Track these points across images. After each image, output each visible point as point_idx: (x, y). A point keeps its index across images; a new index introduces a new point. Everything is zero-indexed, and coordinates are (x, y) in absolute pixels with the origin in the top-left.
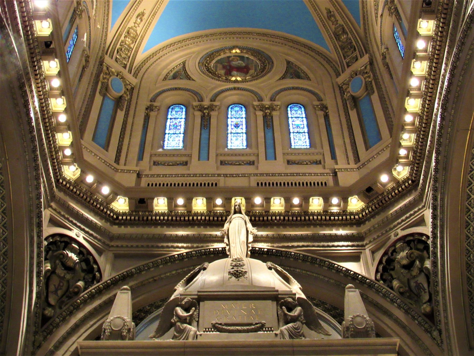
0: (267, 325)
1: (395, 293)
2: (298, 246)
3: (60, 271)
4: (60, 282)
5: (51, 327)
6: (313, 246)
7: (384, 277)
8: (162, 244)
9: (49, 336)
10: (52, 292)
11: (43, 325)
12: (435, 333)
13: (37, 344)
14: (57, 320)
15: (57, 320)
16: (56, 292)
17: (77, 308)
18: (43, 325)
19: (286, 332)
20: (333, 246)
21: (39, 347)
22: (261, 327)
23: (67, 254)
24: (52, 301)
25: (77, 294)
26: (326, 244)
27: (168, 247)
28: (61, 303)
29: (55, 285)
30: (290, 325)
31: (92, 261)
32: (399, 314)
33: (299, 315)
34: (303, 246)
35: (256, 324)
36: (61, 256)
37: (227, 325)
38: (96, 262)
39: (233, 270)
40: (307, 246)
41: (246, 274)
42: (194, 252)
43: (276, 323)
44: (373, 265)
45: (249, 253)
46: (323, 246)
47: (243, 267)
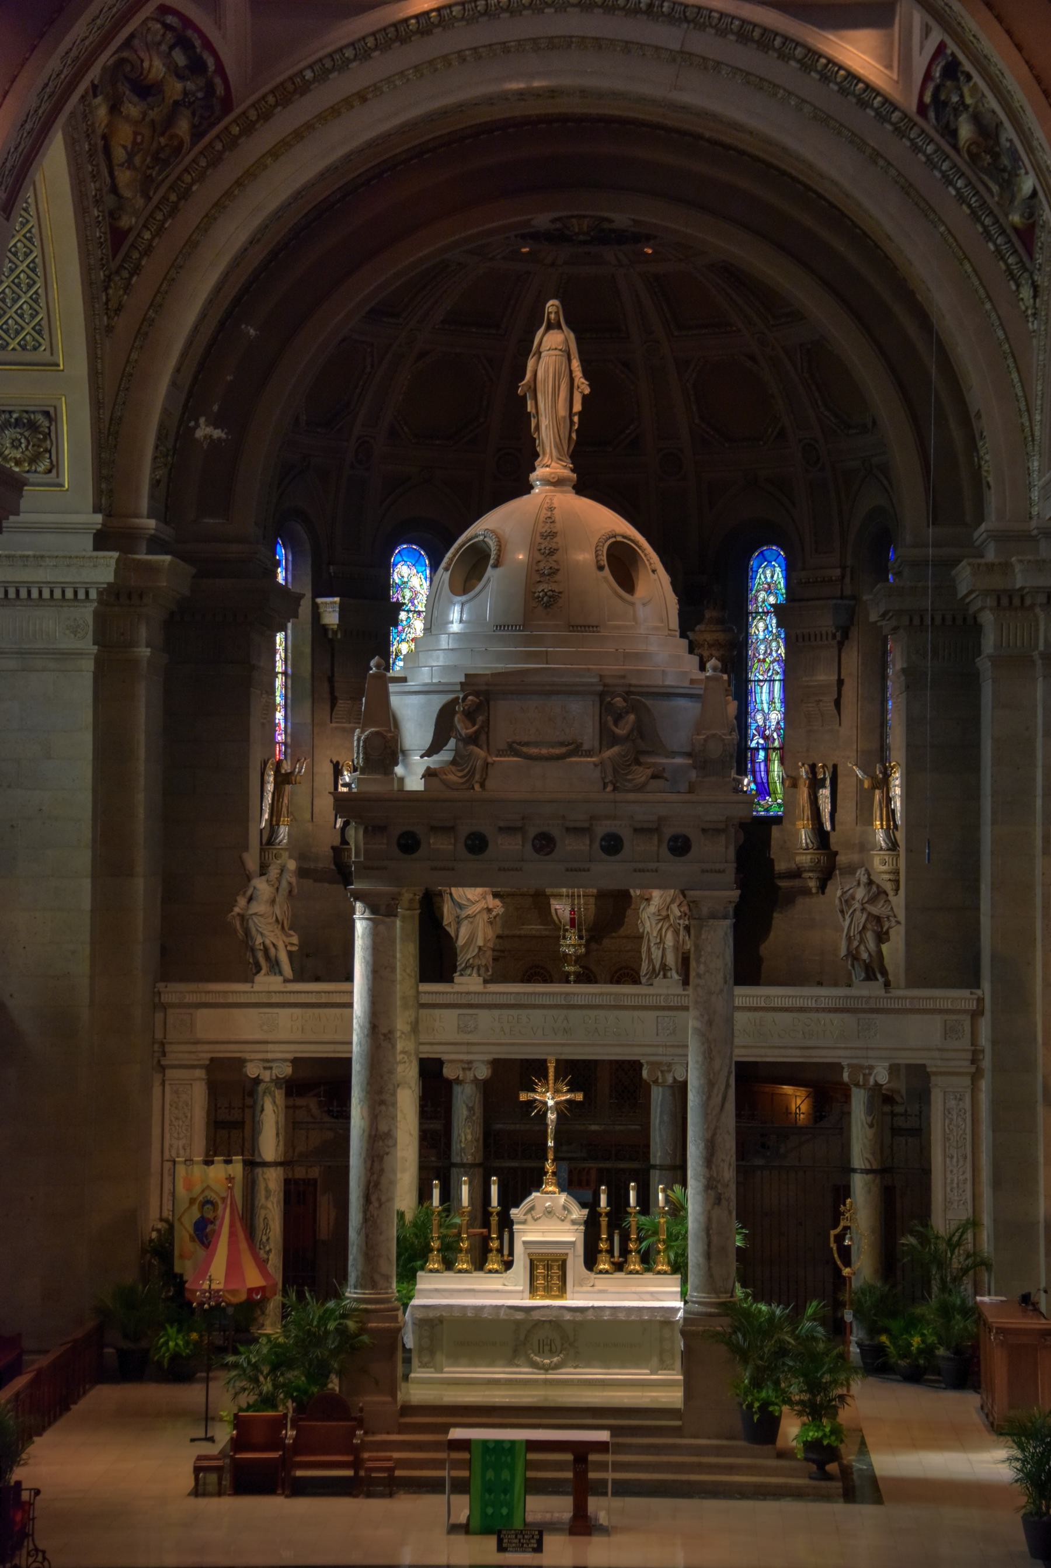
0: (586, 747)
3: (133, 109)
4: (136, 134)
5: (136, 255)
10: (122, 165)
11: (115, 252)
12: (1026, 293)
13: (113, 305)
15: (147, 235)
16: (129, 163)
17: (185, 195)
18: (115, 252)
21: (118, 310)
22: (577, 749)
24: (127, 193)
25: (178, 150)
28: (146, 185)
29: (124, 147)
30: (616, 749)
31: (198, 43)
33: (631, 731)
35: (569, 744)
36: (128, 68)
37: (527, 744)
38: (208, 45)
41: (560, 597)
42: (459, 8)
43: (597, 744)
44: (922, 48)
45: (574, 436)
47: (557, 577)
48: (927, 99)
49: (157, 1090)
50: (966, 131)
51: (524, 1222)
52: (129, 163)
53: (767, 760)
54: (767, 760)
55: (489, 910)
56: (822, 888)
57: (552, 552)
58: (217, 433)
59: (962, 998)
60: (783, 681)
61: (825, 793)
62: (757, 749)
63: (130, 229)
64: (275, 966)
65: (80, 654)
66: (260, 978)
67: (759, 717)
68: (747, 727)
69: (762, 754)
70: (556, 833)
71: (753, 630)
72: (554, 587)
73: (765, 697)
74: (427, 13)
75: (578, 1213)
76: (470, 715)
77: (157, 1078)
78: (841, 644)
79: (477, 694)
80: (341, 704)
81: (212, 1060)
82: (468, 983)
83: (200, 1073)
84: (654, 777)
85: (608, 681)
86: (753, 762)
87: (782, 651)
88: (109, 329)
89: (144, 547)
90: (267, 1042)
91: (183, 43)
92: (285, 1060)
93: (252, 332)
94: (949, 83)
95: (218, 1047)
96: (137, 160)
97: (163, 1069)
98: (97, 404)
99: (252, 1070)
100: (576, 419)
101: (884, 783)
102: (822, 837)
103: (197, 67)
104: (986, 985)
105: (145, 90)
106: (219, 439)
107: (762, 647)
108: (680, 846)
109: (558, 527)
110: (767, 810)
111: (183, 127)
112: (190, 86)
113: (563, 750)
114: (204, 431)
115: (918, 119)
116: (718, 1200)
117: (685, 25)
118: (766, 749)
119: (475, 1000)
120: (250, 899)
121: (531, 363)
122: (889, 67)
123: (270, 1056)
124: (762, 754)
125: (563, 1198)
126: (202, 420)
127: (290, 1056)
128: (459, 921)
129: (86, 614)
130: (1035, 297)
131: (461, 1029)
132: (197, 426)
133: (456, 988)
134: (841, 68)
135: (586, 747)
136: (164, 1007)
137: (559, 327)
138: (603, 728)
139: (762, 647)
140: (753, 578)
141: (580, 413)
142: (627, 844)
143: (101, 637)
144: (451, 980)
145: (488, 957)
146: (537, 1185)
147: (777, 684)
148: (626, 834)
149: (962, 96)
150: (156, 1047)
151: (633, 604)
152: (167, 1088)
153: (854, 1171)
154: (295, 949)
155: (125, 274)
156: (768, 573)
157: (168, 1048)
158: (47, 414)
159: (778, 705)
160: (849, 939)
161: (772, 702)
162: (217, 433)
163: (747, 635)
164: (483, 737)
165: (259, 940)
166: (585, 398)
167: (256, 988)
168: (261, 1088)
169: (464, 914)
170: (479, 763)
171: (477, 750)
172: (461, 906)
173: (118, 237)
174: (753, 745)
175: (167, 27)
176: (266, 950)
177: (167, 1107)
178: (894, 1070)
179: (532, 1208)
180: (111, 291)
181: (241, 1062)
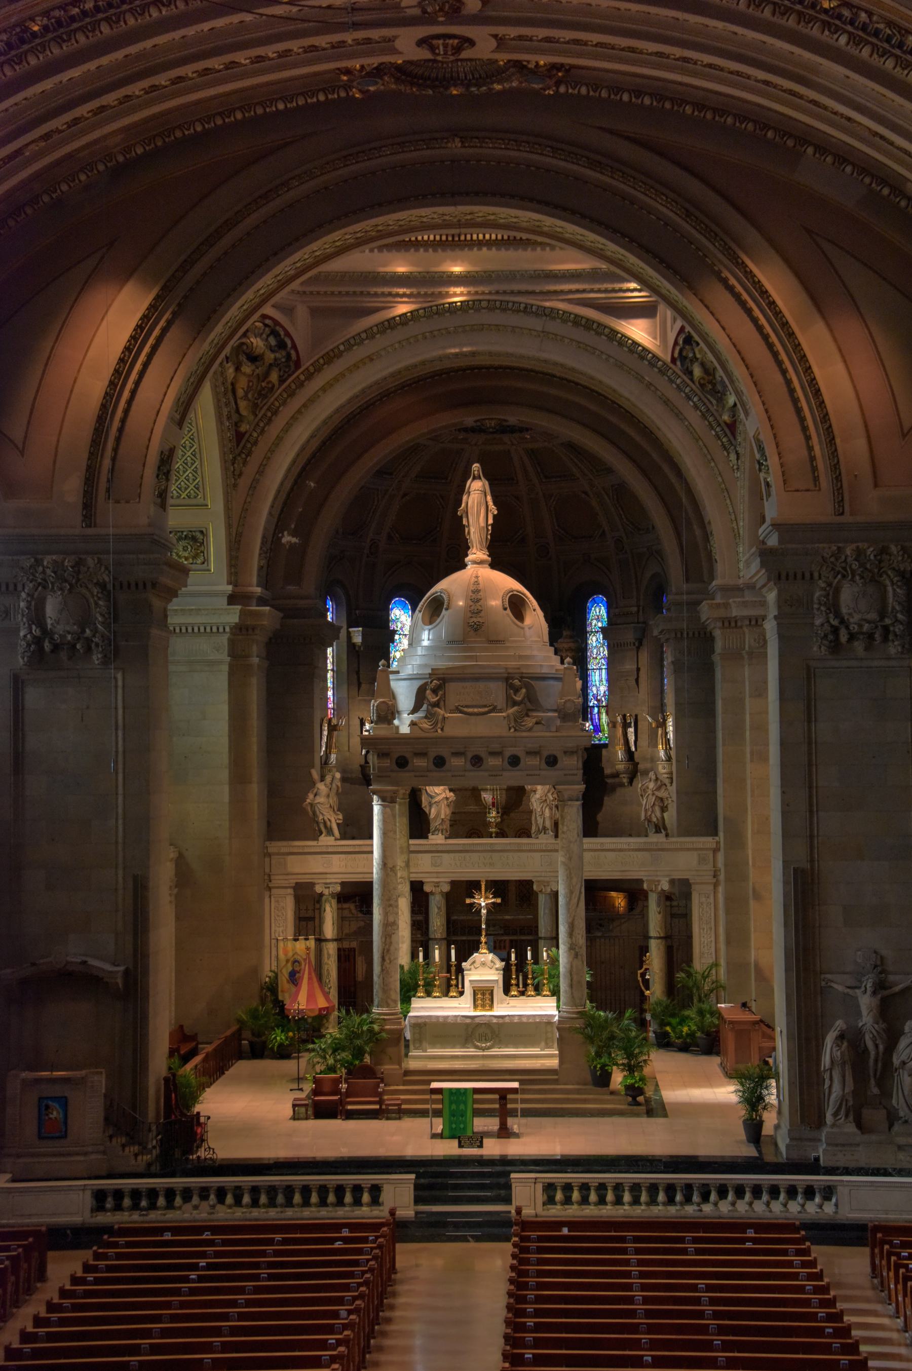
0: (499, 708)
1: (693, 387)
2: (570, 292)
3: (247, 368)
4: (249, 381)
5: (249, 445)
6: (592, 291)
7: (684, 354)
8: (375, 290)
9: (249, 458)
11: (238, 446)
12: (733, 457)
14: (255, 435)
17: (275, 413)
19: (512, 717)
20: (621, 290)
21: (240, 475)
22: (494, 709)
23: (252, 343)
24: (244, 413)
25: (272, 389)
26: (610, 286)
27: (383, 294)
28: (255, 408)
29: (243, 389)
30: (516, 708)
31: (282, 333)
32: (694, 417)
33: (523, 699)
34: (578, 291)
38: (288, 334)
39: (472, 620)
40: (584, 291)
43: (505, 706)
44: (672, 328)
46: (606, 291)
48: (676, 355)
49: (267, 900)
50: (697, 372)
51: (470, 970)
52: (245, 397)
53: (599, 713)
54: (599, 713)
55: (447, 799)
56: (631, 782)
57: (478, 600)
58: (294, 540)
59: (708, 842)
60: (607, 669)
61: (631, 730)
62: (593, 707)
63: (246, 433)
64: (330, 832)
65: (220, 662)
66: (322, 838)
67: (594, 689)
68: (587, 695)
69: (596, 710)
70: (483, 755)
71: (590, 642)
72: (479, 619)
73: (597, 678)
74: (405, 314)
75: (500, 964)
76: (435, 691)
77: (267, 894)
78: (638, 648)
79: (438, 679)
80: (363, 686)
81: (297, 883)
82: (436, 839)
83: (291, 891)
84: (537, 723)
85: (510, 671)
86: (591, 714)
87: (606, 652)
88: (235, 486)
89: (254, 601)
90: (326, 874)
91: (274, 333)
92: (336, 883)
93: (312, 484)
94: (687, 347)
95: (299, 876)
96: (250, 396)
97: (270, 889)
98: (229, 526)
99: (319, 889)
100: (490, 528)
101: (663, 724)
102: (630, 755)
103: (281, 345)
104: (721, 834)
105: (254, 359)
106: (295, 543)
107: (595, 651)
108: (552, 761)
109: (481, 587)
110: (599, 740)
111: (274, 377)
112: (278, 355)
113: (486, 709)
114: (287, 539)
115: (672, 365)
116: (576, 955)
117: (544, 318)
118: (598, 707)
119: (440, 848)
120: (315, 795)
121: (465, 497)
122: (655, 338)
123: (328, 881)
124: (596, 710)
125: (491, 956)
126: (286, 533)
127: (339, 881)
128: (431, 805)
129: (224, 640)
130: (738, 459)
131: (434, 865)
132: (283, 536)
133: (430, 842)
134: (629, 339)
135: (499, 708)
136: (270, 855)
137: (480, 478)
138: (508, 697)
139: (595, 651)
140: (589, 613)
141: (492, 525)
142: (522, 761)
143: (232, 654)
144: (427, 838)
145: (447, 825)
146: (477, 949)
147: (604, 671)
148: (521, 755)
149: (694, 353)
150: (266, 877)
151: (523, 628)
152: (273, 899)
153: (651, 938)
154: (340, 822)
155: (244, 456)
156: (597, 610)
157: (272, 877)
158: (202, 532)
159: (604, 682)
160: (646, 811)
161: (601, 681)
162: (294, 540)
163: (587, 644)
164: (442, 703)
165: (321, 817)
166: (495, 517)
167: (320, 844)
168: (324, 898)
169: (434, 801)
170: (440, 717)
171: (439, 710)
172: (432, 797)
173: (239, 436)
174: (591, 704)
175: (266, 325)
176: (325, 823)
177: (273, 909)
178: (672, 882)
179: (474, 962)
180: (236, 465)
181: (312, 885)
